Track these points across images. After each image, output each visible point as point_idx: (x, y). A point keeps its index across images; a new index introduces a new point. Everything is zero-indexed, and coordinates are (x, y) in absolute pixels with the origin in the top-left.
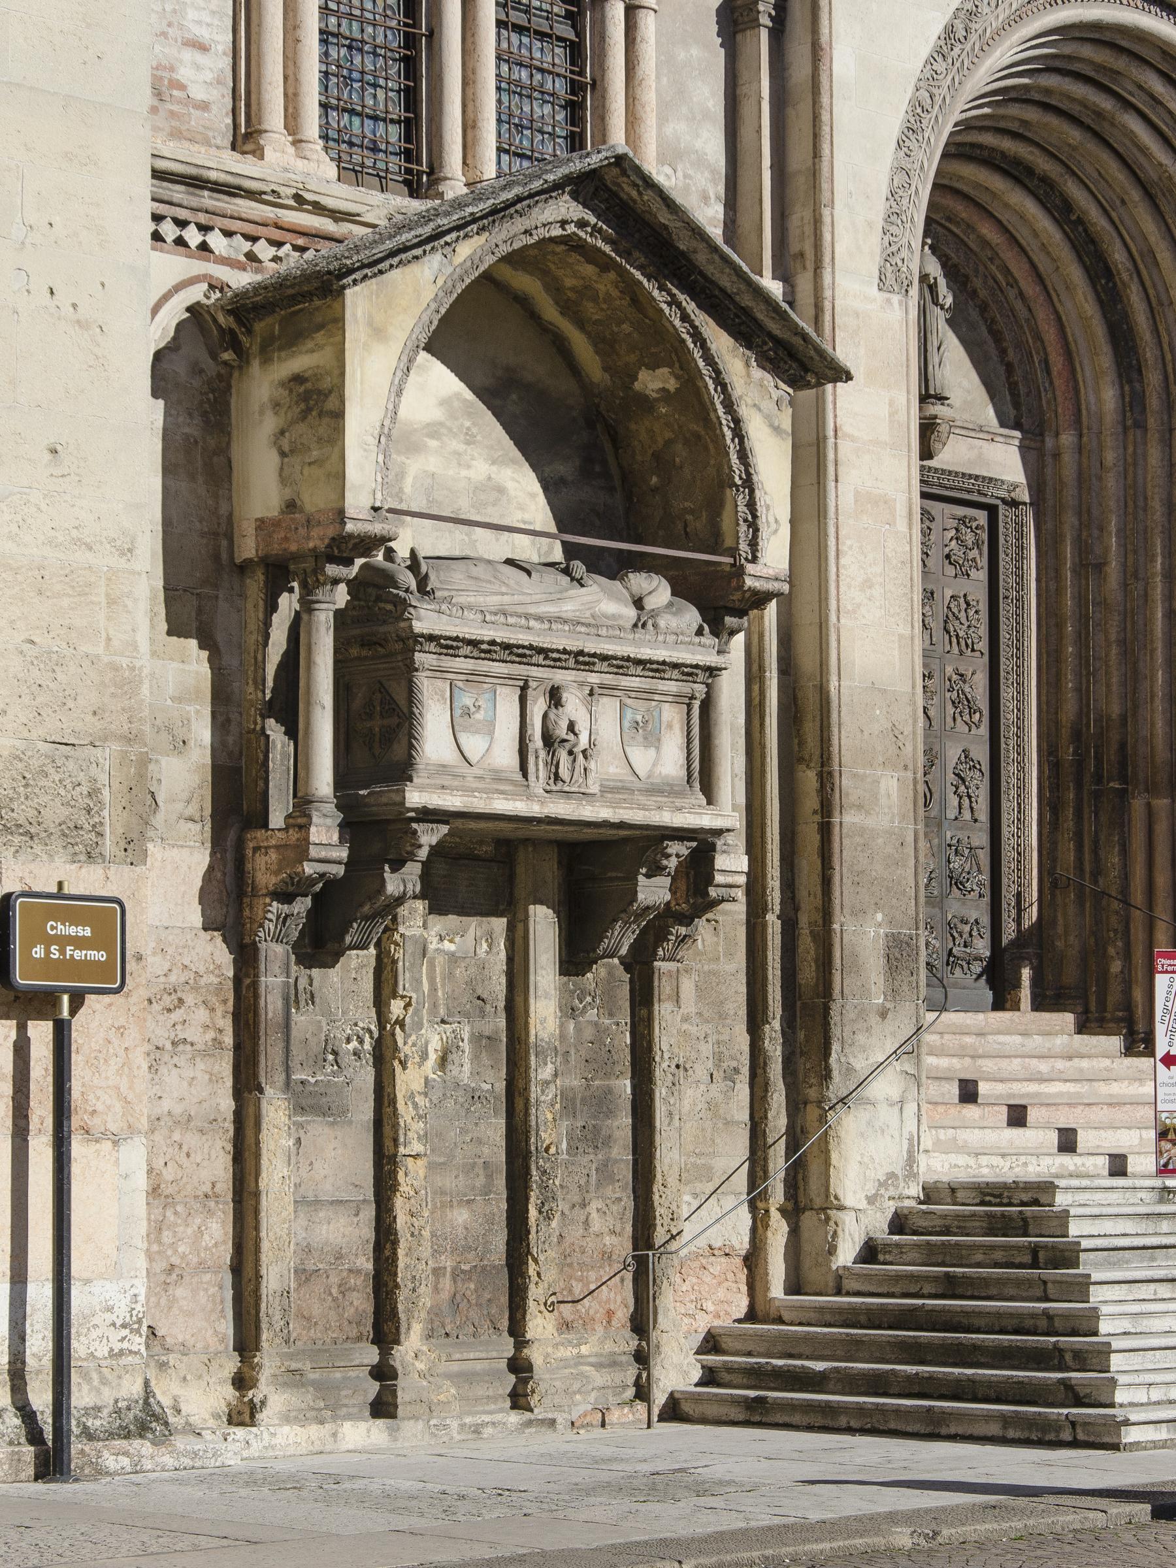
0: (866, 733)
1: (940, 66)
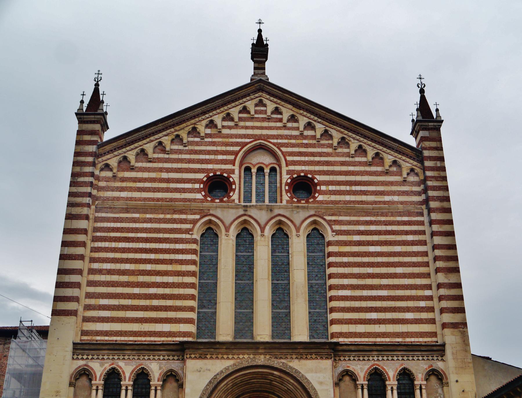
1: (208, 387)
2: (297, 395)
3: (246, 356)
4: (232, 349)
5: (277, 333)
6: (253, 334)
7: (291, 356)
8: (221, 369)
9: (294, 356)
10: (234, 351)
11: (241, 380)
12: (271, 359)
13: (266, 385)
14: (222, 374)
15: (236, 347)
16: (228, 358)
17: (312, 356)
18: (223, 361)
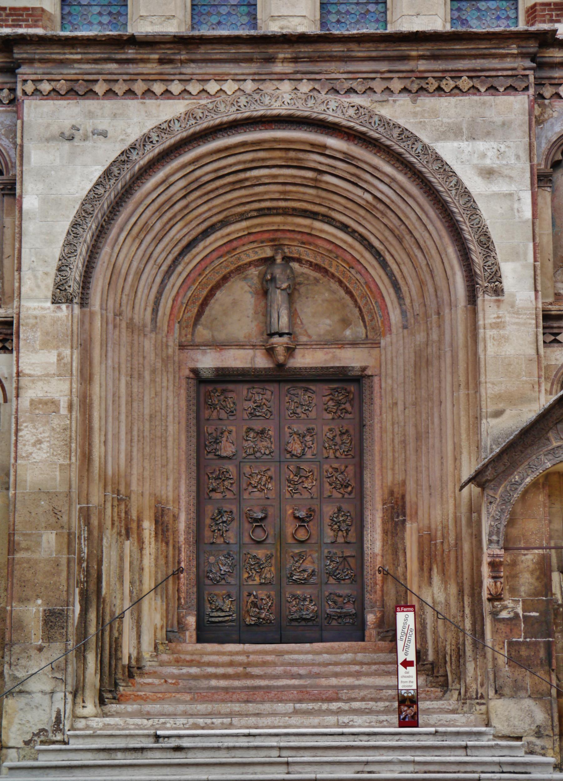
0: (33, 514)
1: (101, 190)
2: (408, 217)
3: (230, 87)
4: (182, 62)
5: (338, 12)
6: (255, 18)
7: (385, 84)
8: (145, 131)
9: (396, 85)
10: (188, 71)
11: (216, 171)
12: (315, 93)
13: (302, 189)
14: (149, 147)
15: (193, 57)
16: (167, 93)
17: (460, 83)
18: (150, 102)
